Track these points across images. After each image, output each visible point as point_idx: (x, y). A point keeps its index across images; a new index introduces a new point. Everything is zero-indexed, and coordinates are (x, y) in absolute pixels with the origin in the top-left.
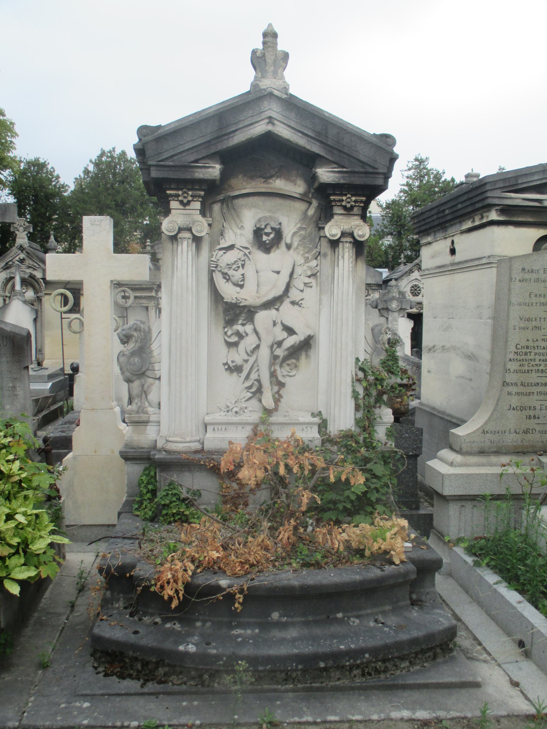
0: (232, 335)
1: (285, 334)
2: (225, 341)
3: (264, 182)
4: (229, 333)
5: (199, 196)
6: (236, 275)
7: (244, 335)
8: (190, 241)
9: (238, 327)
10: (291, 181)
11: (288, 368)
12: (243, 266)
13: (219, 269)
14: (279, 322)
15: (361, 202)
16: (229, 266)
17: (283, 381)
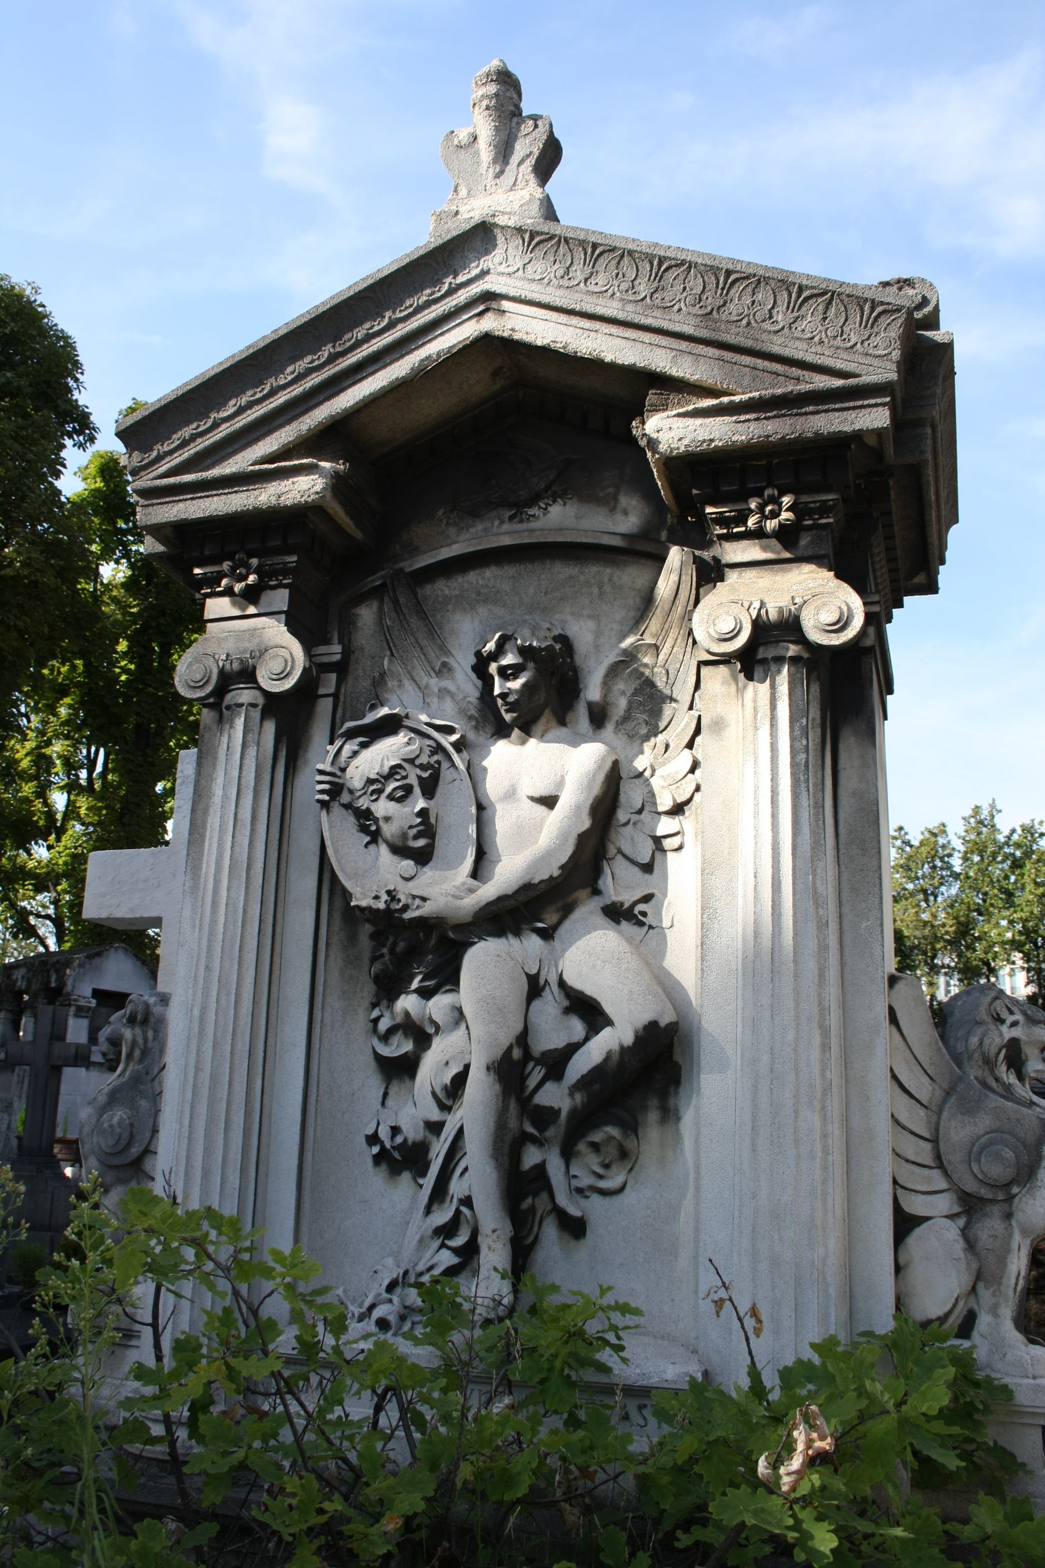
0: (392, 1031)
1: (577, 1028)
2: (379, 1058)
3: (511, 518)
4: (384, 1025)
5: (286, 572)
6: (395, 815)
7: (431, 1030)
8: (256, 714)
9: (408, 1003)
10: (598, 501)
11: (594, 1161)
12: (429, 788)
13: (345, 798)
14: (553, 980)
15: (824, 509)
16: (376, 785)
17: (574, 1211)
